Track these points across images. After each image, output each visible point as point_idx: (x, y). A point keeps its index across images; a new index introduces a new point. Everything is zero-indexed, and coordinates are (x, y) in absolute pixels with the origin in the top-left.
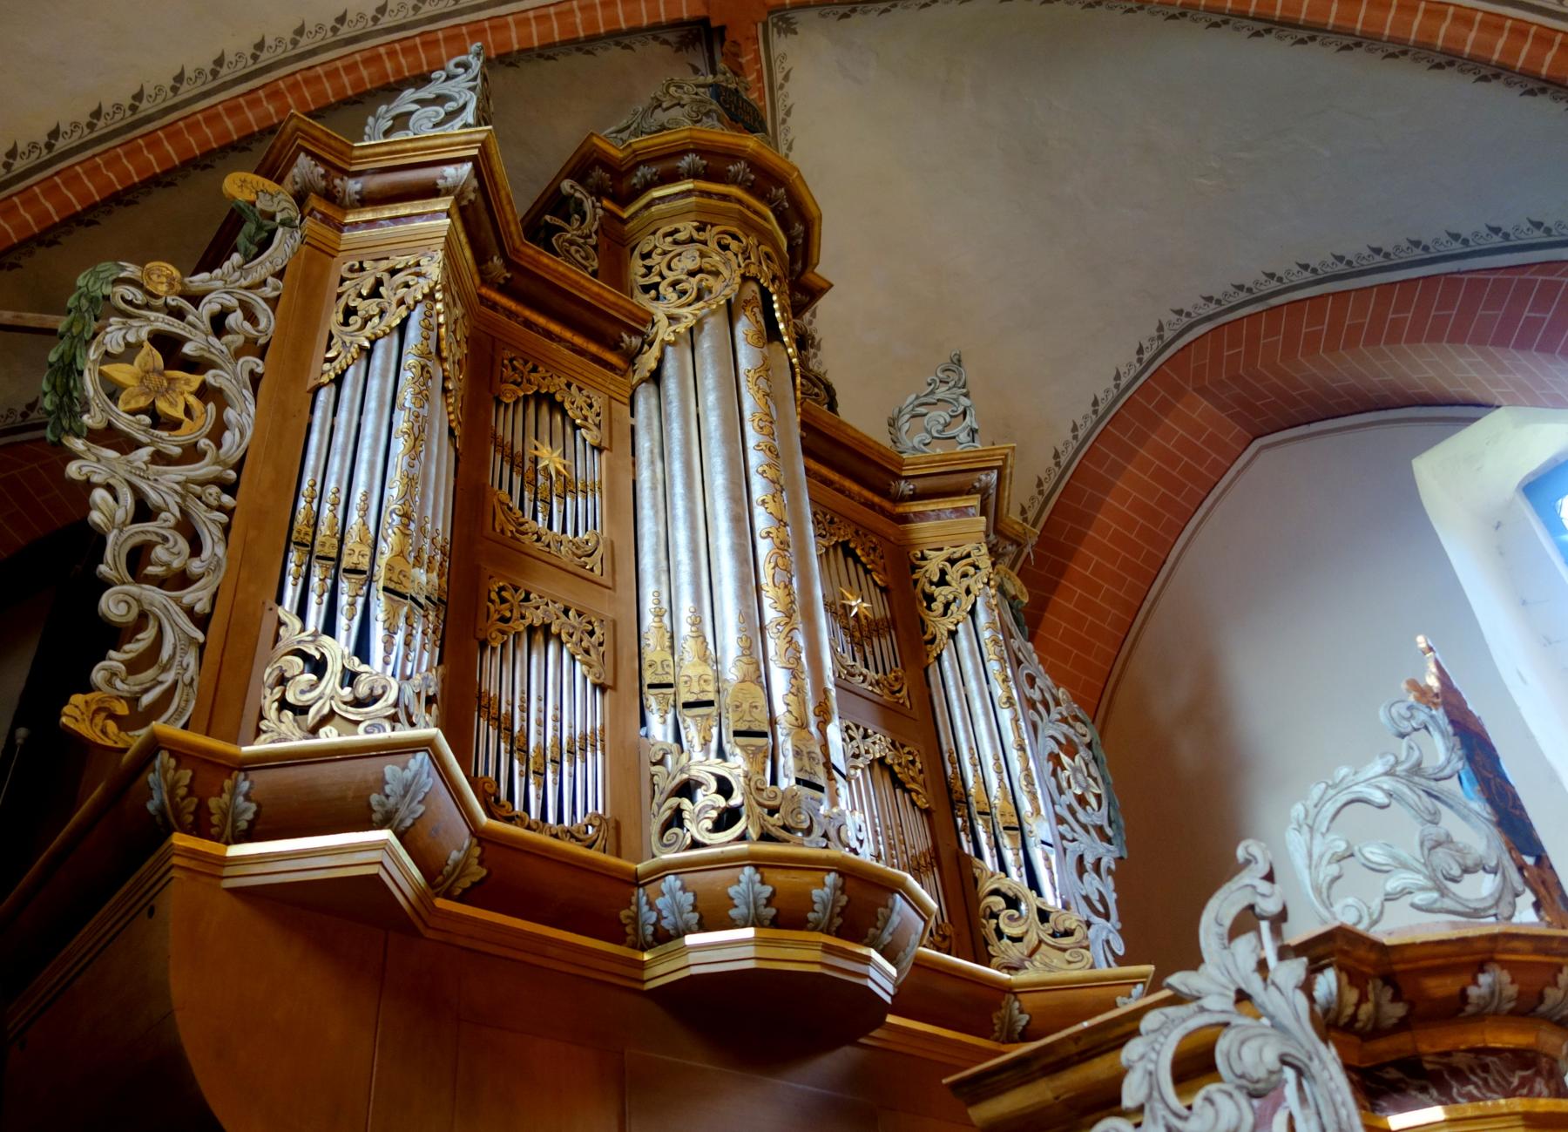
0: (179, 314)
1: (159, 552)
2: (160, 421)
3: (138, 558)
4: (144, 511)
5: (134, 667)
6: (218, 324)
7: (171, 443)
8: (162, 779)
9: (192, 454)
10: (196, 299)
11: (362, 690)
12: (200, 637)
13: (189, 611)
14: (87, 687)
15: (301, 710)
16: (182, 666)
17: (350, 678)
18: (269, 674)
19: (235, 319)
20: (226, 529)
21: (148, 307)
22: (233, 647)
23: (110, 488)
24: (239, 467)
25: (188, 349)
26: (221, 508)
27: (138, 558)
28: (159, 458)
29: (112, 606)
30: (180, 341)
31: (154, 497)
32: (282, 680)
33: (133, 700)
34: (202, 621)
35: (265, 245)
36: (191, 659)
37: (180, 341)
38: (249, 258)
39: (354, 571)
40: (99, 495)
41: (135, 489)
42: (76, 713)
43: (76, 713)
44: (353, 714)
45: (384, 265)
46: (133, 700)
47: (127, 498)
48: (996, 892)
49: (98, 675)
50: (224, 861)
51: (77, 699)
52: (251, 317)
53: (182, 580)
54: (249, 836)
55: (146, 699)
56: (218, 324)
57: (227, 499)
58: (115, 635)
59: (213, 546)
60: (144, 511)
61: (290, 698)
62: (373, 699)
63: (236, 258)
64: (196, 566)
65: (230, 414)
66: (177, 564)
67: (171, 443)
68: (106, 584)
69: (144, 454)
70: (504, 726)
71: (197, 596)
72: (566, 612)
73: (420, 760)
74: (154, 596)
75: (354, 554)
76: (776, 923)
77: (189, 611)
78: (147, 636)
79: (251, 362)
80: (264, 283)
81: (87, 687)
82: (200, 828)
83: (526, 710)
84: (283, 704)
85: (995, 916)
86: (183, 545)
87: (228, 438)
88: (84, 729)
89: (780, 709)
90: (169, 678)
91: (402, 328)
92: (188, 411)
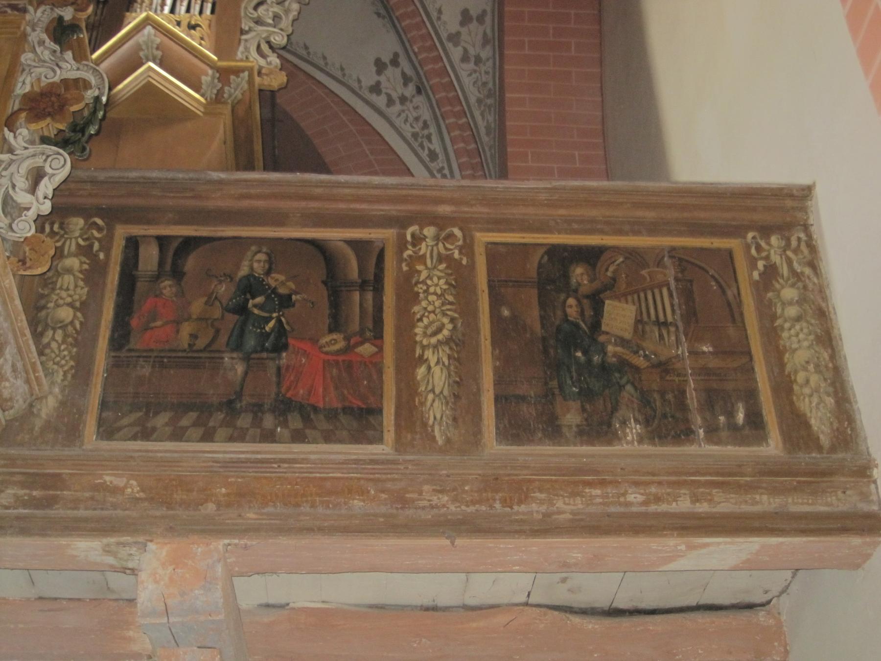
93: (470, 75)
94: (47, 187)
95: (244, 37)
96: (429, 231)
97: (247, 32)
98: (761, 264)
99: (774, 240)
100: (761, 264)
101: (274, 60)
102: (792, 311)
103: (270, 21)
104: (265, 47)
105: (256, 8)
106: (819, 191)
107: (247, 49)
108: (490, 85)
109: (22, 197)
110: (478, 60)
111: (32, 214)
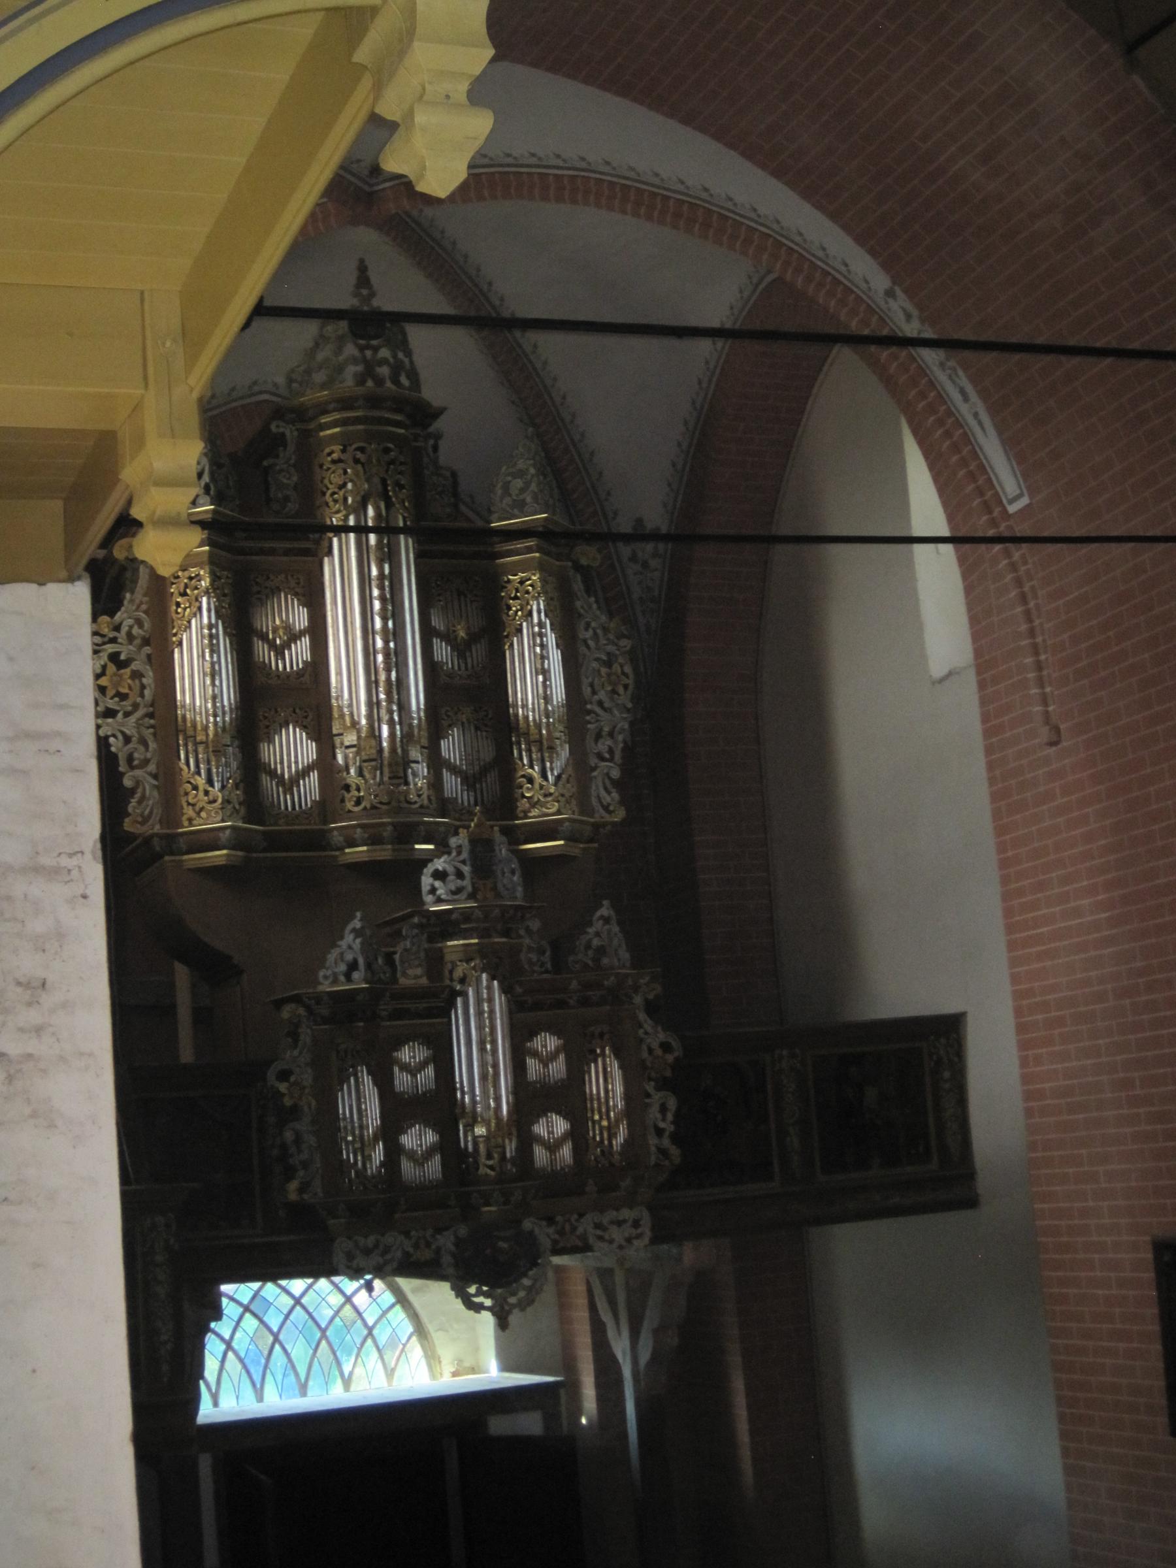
0: (113, 640)
1: (136, 755)
2: (123, 697)
3: (130, 759)
4: (127, 739)
5: (139, 802)
6: (130, 637)
7: (127, 705)
8: (157, 845)
9: (136, 706)
10: (117, 628)
11: (211, 798)
12: (156, 783)
13: (150, 774)
14: (128, 815)
15: (193, 805)
16: (153, 796)
17: (206, 793)
18: (182, 793)
19: (136, 631)
20: (155, 735)
21: (104, 643)
22: (168, 779)
23: (114, 736)
24: (152, 705)
25: (123, 657)
26: (152, 727)
27: (130, 759)
28: (127, 714)
29: (127, 782)
30: (118, 654)
31: (128, 732)
32: (187, 794)
33: (142, 815)
34: (155, 777)
35: (135, 581)
36: (156, 793)
37: (118, 654)
38: (132, 592)
39: (202, 743)
40: (112, 740)
41: (123, 733)
42: (128, 825)
43: (128, 825)
44: (209, 807)
45: (186, 574)
46: (142, 815)
47: (120, 737)
48: (523, 776)
49: (130, 809)
50: (182, 861)
51: (127, 820)
52: (141, 626)
53: (146, 762)
54: (188, 853)
55: (147, 812)
56: (130, 637)
57: (152, 722)
58: (132, 791)
59: (152, 745)
60: (127, 739)
61: (191, 801)
62: (214, 801)
63: (128, 595)
64: (149, 755)
65: (144, 681)
66: (142, 757)
67: (127, 705)
68: (122, 774)
69: (120, 715)
70: (273, 774)
71: (152, 767)
72: (294, 712)
73: (228, 832)
74: (138, 773)
75: (200, 737)
76: (373, 844)
77: (150, 774)
78: (140, 790)
79: (147, 650)
80: (141, 603)
81: (128, 815)
82: (172, 853)
83: (282, 762)
84: (189, 804)
85: (521, 787)
86: (142, 748)
87: (147, 692)
88: (131, 830)
89: (385, 744)
90: (151, 802)
91: (200, 609)
92: (130, 688)
93: (635, 574)
94: (670, 1116)
95: (595, 774)
96: (785, 1052)
97: (594, 769)
98: (935, 1057)
99: (943, 1041)
100: (935, 1057)
101: (615, 795)
102: (947, 1086)
103: (607, 756)
104: (607, 782)
105: (596, 741)
106: (970, 1020)
107: (597, 788)
108: (656, 593)
109: (662, 1125)
110: (645, 565)
111: (667, 1133)
